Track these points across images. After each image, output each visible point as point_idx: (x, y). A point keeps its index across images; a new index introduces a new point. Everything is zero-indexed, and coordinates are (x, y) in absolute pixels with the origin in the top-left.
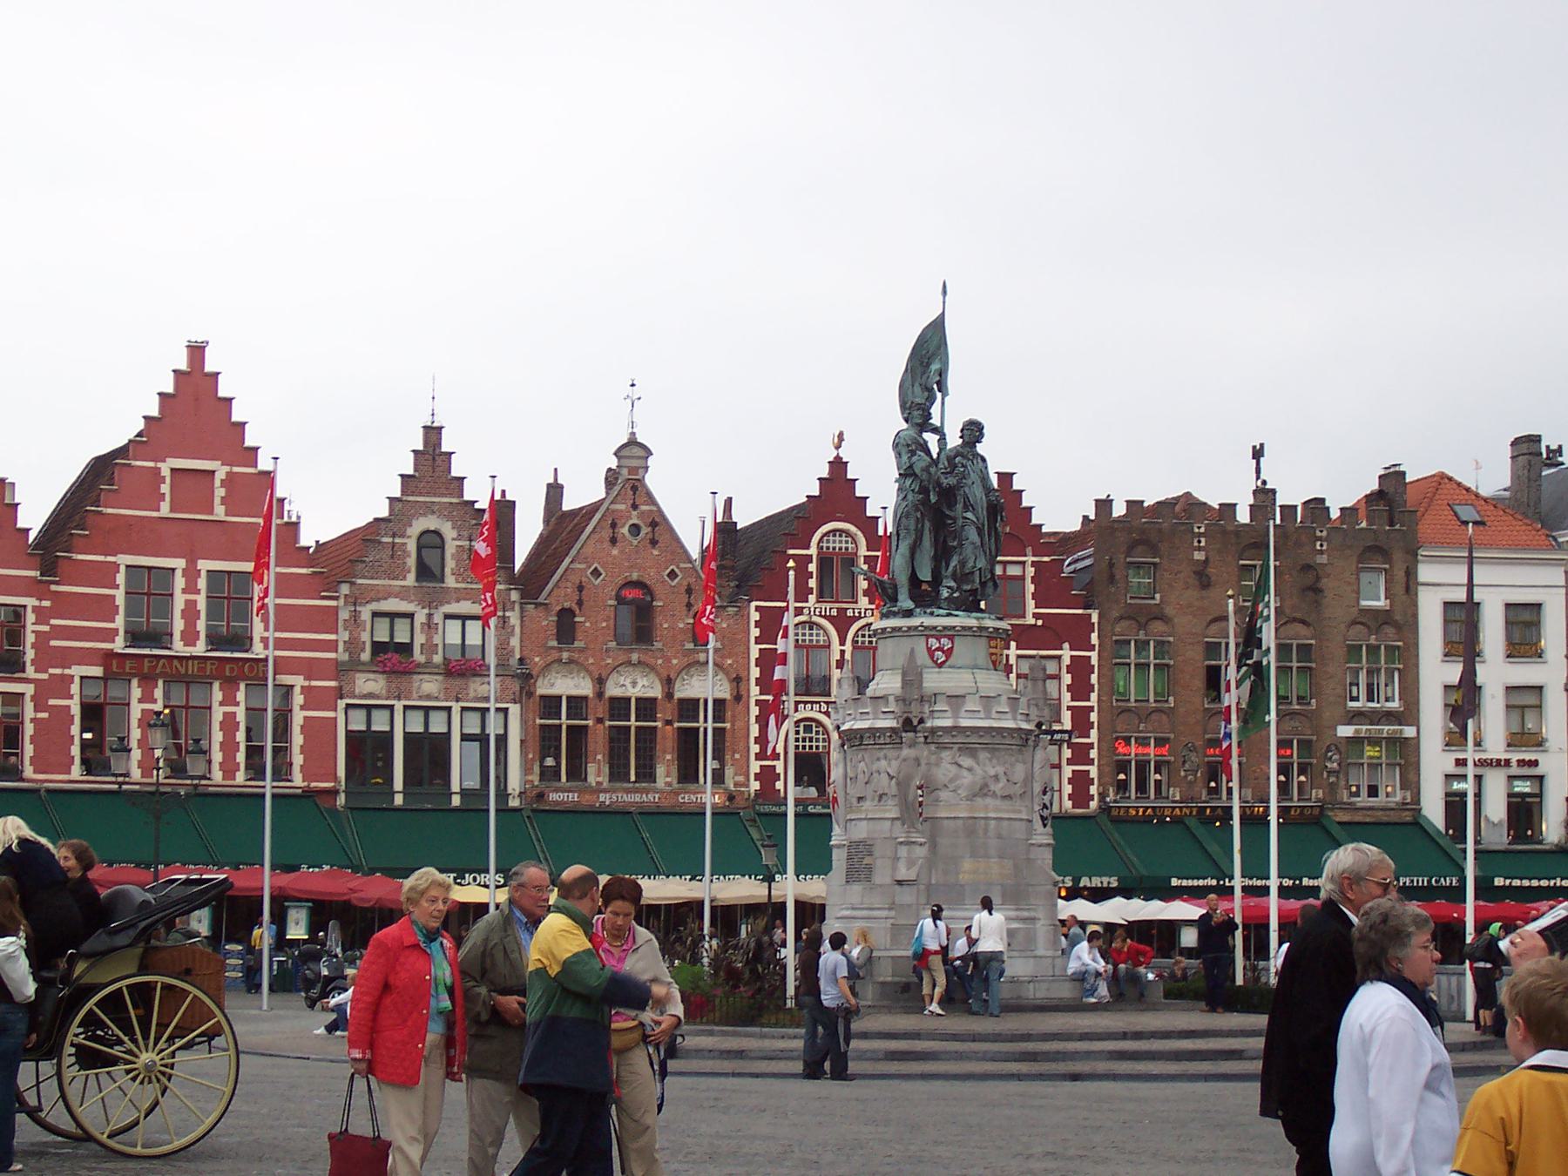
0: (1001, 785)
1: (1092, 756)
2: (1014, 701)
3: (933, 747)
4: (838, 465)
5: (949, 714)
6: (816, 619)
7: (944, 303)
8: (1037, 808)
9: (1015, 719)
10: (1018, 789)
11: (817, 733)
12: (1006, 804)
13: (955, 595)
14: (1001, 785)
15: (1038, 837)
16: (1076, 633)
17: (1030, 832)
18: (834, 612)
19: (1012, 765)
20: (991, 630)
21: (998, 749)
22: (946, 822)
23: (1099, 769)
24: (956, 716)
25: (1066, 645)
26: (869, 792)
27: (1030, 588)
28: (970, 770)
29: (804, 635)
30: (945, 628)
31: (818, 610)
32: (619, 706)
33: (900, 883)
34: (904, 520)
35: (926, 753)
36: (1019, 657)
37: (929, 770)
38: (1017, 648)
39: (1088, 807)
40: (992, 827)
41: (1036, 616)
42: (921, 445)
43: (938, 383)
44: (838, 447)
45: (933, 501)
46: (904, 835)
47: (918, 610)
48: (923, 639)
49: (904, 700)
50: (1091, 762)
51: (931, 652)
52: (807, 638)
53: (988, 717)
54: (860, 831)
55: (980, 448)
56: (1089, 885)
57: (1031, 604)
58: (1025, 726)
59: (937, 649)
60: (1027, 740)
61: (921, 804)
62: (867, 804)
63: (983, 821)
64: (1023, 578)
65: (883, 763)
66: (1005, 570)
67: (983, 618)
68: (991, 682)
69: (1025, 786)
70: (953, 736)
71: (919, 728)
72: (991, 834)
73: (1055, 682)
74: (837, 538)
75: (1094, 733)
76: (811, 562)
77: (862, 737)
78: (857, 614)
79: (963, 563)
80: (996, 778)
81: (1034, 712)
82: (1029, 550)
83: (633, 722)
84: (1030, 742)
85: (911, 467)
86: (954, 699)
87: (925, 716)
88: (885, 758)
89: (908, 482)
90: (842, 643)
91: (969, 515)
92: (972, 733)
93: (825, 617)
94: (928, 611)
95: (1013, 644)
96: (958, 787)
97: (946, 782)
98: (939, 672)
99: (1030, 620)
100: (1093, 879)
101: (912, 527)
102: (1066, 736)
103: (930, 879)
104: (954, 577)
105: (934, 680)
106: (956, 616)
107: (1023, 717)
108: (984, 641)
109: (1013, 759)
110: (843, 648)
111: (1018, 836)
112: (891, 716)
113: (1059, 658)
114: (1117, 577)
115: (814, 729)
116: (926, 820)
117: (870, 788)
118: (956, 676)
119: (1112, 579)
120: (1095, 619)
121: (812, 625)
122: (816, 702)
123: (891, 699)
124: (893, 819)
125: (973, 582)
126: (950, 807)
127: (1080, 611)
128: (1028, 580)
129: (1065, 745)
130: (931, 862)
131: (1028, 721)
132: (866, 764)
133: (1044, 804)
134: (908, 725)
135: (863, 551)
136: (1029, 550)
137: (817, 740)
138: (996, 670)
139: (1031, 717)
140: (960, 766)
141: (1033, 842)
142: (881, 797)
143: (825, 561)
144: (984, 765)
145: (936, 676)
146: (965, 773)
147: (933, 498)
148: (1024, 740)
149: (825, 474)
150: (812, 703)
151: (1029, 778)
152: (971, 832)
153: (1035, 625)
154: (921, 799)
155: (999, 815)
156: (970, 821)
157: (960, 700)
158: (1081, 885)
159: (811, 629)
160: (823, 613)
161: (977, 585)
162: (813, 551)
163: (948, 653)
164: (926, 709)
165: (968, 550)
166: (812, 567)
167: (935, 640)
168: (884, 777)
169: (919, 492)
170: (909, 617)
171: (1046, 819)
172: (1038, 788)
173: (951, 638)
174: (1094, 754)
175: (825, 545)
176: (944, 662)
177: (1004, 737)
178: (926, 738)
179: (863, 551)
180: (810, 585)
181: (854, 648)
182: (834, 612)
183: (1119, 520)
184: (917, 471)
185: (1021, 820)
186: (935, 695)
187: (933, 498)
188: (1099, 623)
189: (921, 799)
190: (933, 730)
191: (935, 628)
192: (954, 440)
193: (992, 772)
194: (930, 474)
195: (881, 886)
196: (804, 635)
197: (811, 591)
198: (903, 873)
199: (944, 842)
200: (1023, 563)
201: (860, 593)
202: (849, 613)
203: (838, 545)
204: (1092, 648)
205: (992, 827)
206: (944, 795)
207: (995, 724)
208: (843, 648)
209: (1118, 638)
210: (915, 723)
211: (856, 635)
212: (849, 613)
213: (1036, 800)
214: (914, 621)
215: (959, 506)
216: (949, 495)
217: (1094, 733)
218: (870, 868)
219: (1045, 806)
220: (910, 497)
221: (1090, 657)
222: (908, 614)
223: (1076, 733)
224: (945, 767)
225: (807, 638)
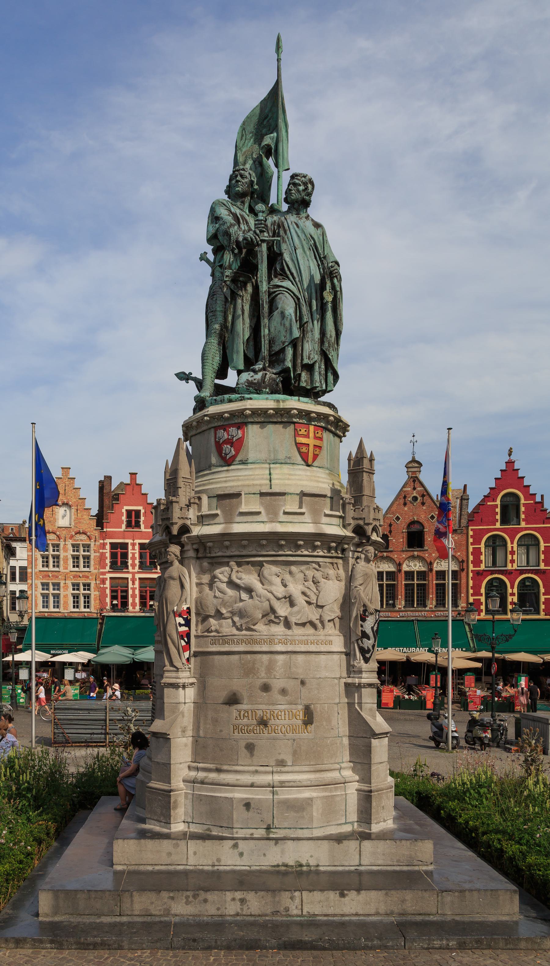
0: (295, 609)
5: (220, 519)
22: (216, 657)
28: (249, 590)
32: (409, 575)
40: (280, 663)
53: (273, 518)
60: (343, 551)
63: (265, 657)
76: (497, 508)
81: (350, 512)
83: (416, 582)
87: (188, 522)
90: (512, 543)
98: (227, 470)
109: (318, 575)
143: (504, 508)
156: (249, 656)
166: (498, 510)
178: (197, 551)
189: (184, 629)
193: (280, 591)
197: (497, 520)
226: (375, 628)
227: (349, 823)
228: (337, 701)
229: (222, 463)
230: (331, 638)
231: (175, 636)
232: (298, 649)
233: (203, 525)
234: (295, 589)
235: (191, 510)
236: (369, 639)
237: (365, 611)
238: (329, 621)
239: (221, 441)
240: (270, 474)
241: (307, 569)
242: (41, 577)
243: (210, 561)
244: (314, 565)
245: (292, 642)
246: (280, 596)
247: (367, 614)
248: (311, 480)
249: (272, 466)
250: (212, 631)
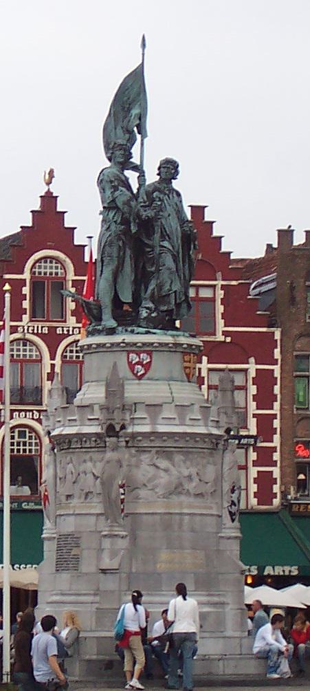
0: (194, 484)
1: (275, 458)
2: (205, 409)
3: (133, 451)
4: (49, 199)
5: (147, 421)
6: (29, 336)
7: (143, 54)
8: (226, 505)
9: (206, 425)
10: (208, 488)
11: (30, 438)
12: (198, 502)
13: (153, 315)
14: (194, 484)
15: (227, 531)
16: (261, 349)
17: (220, 526)
18: (46, 331)
19: (204, 466)
20: (185, 346)
22: (145, 517)
23: (281, 470)
24: (154, 423)
25: (252, 360)
26: (76, 490)
27: (220, 309)
28: (166, 471)
29: (18, 350)
30: (144, 344)
31: (31, 329)
33: (104, 571)
34: (107, 248)
35: (127, 456)
36: (210, 370)
37: (130, 471)
38: (209, 362)
39: (272, 504)
40: (186, 521)
41: (225, 334)
42: (123, 181)
43: (138, 126)
44: (49, 183)
45: (133, 231)
46: (107, 529)
47: (120, 328)
48: (125, 354)
49: (108, 409)
50: (274, 464)
51: (131, 366)
52: (21, 353)
54: (69, 525)
55: (175, 184)
56: (272, 573)
57: (220, 323)
58: (215, 431)
59: (138, 363)
60: (217, 444)
61: (122, 501)
62: (74, 502)
63: (177, 517)
64: (213, 300)
65: (89, 464)
66: (197, 294)
67: (178, 336)
68: (185, 392)
69: (216, 485)
70: (151, 441)
71: (121, 433)
72: (185, 527)
73: (242, 392)
74: (48, 264)
75: (277, 438)
77: (70, 442)
78: (65, 332)
79: (160, 287)
80: (190, 477)
81: (224, 420)
82: (219, 275)
84: (220, 446)
85: (114, 201)
86: (152, 408)
87: (126, 422)
88: (91, 460)
89: (111, 214)
90: (53, 357)
91: (166, 244)
92: (169, 438)
93: (37, 334)
94: (129, 329)
95: (205, 359)
96: (156, 486)
97: (145, 482)
98: (138, 384)
99: (220, 338)
100: (276, 568)
101: (115, 254)
102: (252, 441)
103: (131, 569)
104: (152, 299)
105: (134, 391)
106: (154, 333)
107: (214, 424)
108: (178, 356)
109: (205, 461)
110: (53, 362)
112: (96, 423)
113: (246, 371)
114: (298, 299)
115: (28, 434)
116: (126, 516)
117: (77, 487)
118: (154, 387)
119: (293, 300)
120: (278, 336)
121: (25, 342)
122: (30, 411)
123: (96, 408)
124: (98, 515)
125: (169, 303)
126: (149, 504)
127: (264, 330)
128: (218, 302)
129: (251, 448)
130: (132, 553)
131: (218, 427)
132: (74, 466)
133: (232, 501)
134: (111, 431)
135: (71, 276)
136: (219, 275)
137: (30, 444)
138: (189, 382)
139: (221, 424)
140: (157, 467)
141: (222, 535)
142: (87, 495)
143: (37, 285)
144: (179, 466)
145: (136, 387)
146: (162, 474)
147: (134, 229)
148: (214, 444)
149: (37, 208)
150: (26, 411)
151: (219, 479)
152: (167, 527)
153: (224, 342)
154: (122, 497)
156: (167, 517)
157: (157, 408)
158: (266, 573)
159: (25, 345)
160: (36, 331)
161: (173, 306)
162: (26, 275)
163: (147, 367)
164: (128, 417)
165: (165, 275)
166: (26, 290)
167: (135, 355)
168: (90, 477)
169: (121, 224)
170: (112, 334)
171: (234, 514)
172: (227, 487)
173: (150, 353)
174: (276, 456)
175: (37, 270)
176: (143, 375)
177: (197, 441)
179: (71, 276)
180: (24, 306)
181: (63, 362)
182: (46, 331)
183: (299, 248)
184: (120, 204)
185: (212, 515)
186: (135, 404)
187: (134, 229)
188: (281, 340)
189: (122, 497)
190: (134, 436)
191: (135, 344)
192: (152, 177)
193: (186, 473)
194: (131, 207)
195: (86, 574)
196: (18, 350)
198: (107, 563)
199: (143, 534)
200: (214, 286)
201: (69, 313)
202: (59, 331)
203: (48, 271)
204: (275, 362)
206: (143, 493)
207: (189, 430)
208: (53, 362)
209: (299, 353)
210: (118, 429)
211: (65, 350)
212: (59, 331)
213: (226, 498)
214: (117, 339)
215: (157, 236)
216: (147, 226)
217: (277, 438)
218: (77, 559)
219: (233, 503)
220: (113, 227)
221: (273, 370)
222: (111, 331)
223: (261, 438)
224: (144, 468)
225: (21, 353)
229: (134, 377)
230: (212, 505)
233: (134, 425)
236: (235, 505)
237: (234, 487)
239: (134, 362)
240: (170, 389)
243: (137, 449)
247: (236, 488)
249: (171, 382)
250: (140, 499)
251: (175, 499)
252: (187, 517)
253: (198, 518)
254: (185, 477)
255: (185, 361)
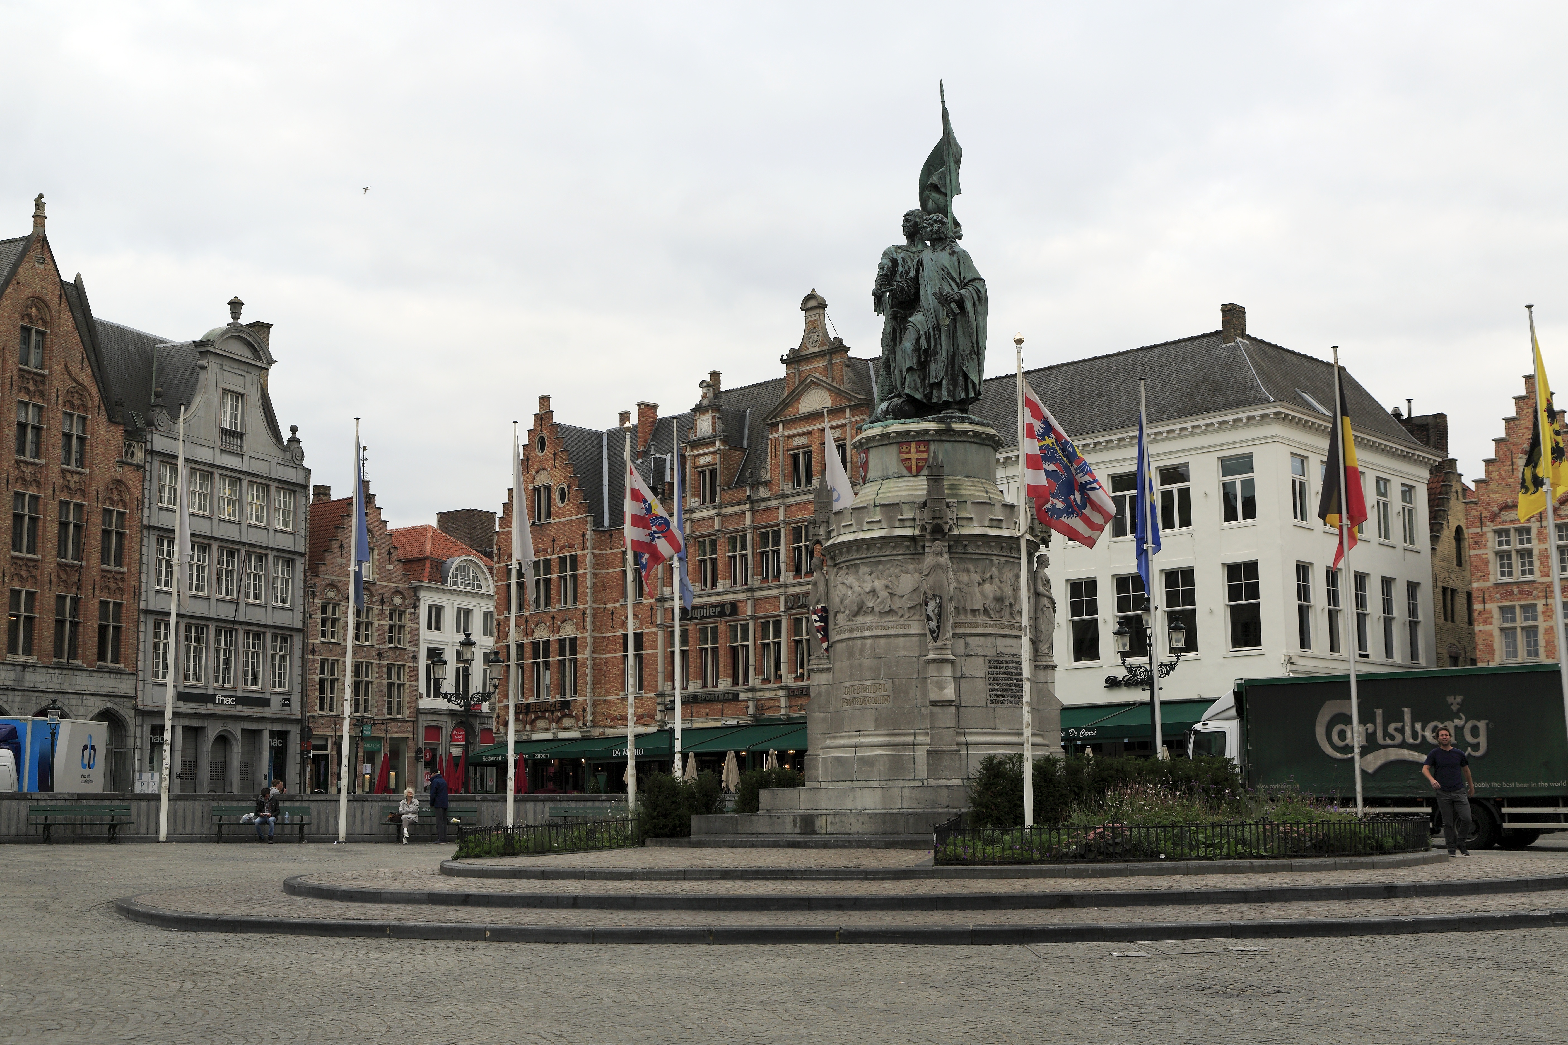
10: (906, 603)
21: (880, 562)
40: (868, 646)
63: (859, 642)
67: (889, 426)
72: (867, 652)
80: (873, 592)
87: (820, 538)
109: (897, 571)
111: (902, 653)
155: (875, 633)
156: (850, 643)
164: (822, 531)
205: (868, 646)
207: (861, 536)
226: (936, 611)
227: (918, 779)
228: (915, 676)
231: (814, 631)
232: (880, 633)
234: (878, 584)
235: (822, 529)
238: (909, 608)
241: (892, 566)
242: (1498, 596)
244: (897, 562)
245: (877, 628)
246: (867, 590)
248: (909, 490)
251: (860, 619)
252: (869, 641)
253: (882, 641)
254: (868, 593)
255: (901, 453)
